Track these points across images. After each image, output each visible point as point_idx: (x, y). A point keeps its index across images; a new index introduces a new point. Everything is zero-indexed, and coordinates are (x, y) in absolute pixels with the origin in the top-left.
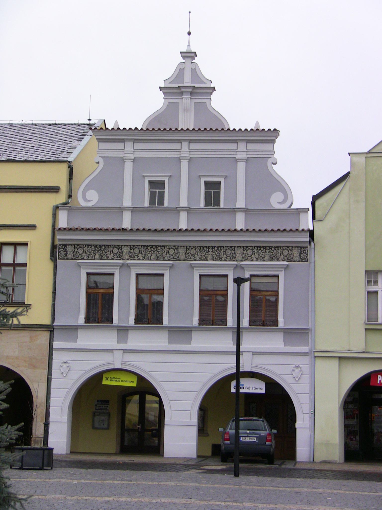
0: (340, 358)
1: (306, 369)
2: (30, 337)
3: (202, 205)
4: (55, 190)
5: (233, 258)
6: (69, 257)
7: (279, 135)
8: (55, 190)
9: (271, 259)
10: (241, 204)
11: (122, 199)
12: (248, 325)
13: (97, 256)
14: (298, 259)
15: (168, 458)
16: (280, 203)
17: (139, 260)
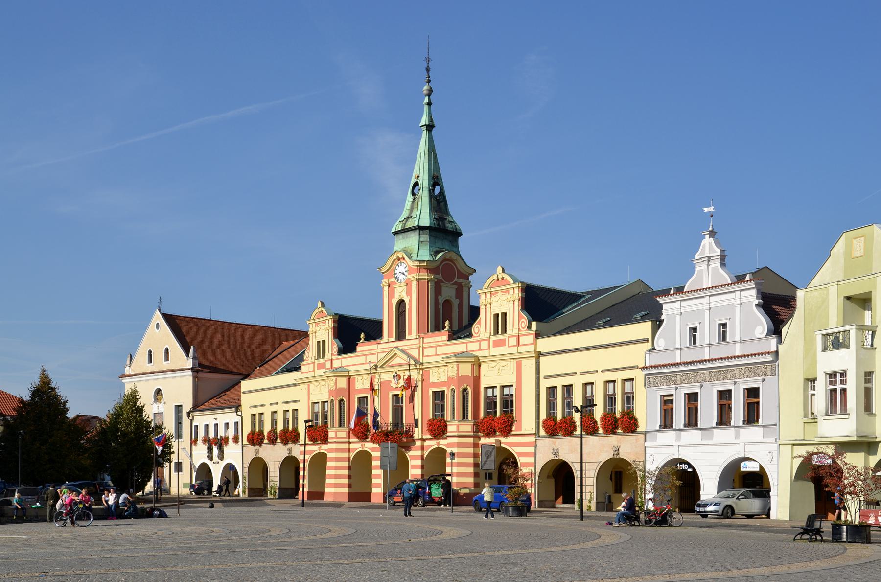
0: (794, 445)
1: (775, 454)
2: (636, 440)
3: (717, 341)
4: (648, 340)
5: (734, 378)
6: (652, 385)
7: (78, 416)
8: (648, 340)
9: (755, 376)
10: (737, 338)
11: (675, 343)
12: (715, 425)
13: (665, 384)
14: (769, 374)
15: (173, 495)
16: (761, 334)
17: (685, 383)
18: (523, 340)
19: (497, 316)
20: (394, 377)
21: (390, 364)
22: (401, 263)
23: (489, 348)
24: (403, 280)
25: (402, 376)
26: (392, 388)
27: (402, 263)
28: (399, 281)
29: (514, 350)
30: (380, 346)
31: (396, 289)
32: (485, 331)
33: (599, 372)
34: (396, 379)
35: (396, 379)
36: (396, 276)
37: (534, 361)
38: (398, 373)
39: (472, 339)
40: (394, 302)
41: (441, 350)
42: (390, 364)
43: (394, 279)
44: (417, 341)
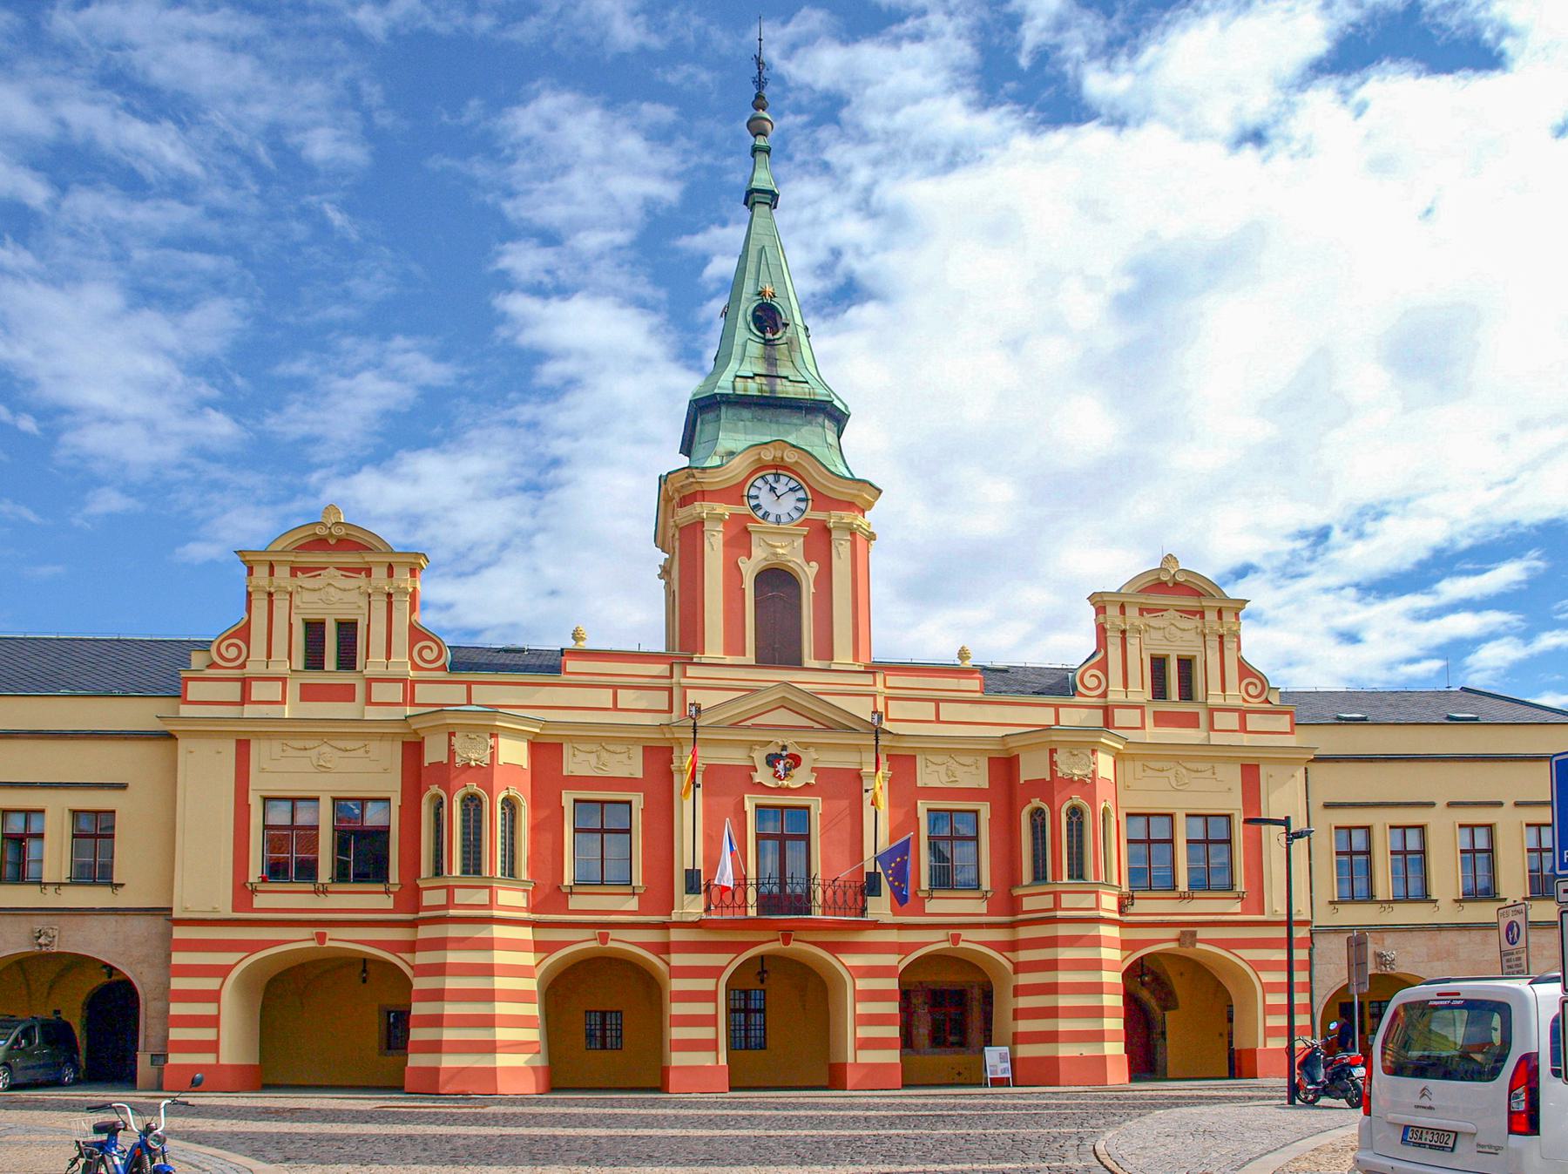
18: (1253, 722)
19: (1159, 664)
20: (772, 760)
21: (748, 723)
22: (777, 477)
23: (1143, 727)
24: (784, 519)
25: (809, 758)
26: (762, 788)
27: (784, 480)
28: (772, 518)
29: (1246, 739)
30: (691, 671)
31: (754, 537)
32: (1126, 685)
33: (1509, 803)
34: (780, 767)
35: (780, 767)
36: (753, 502)
37: (1300, 773)
38: (790, 751)
39: (1078, 699)
40: (749, 569)
41: (947, 711)
42: (748, 723)
43: (745, 510)
44: (868, 679)
